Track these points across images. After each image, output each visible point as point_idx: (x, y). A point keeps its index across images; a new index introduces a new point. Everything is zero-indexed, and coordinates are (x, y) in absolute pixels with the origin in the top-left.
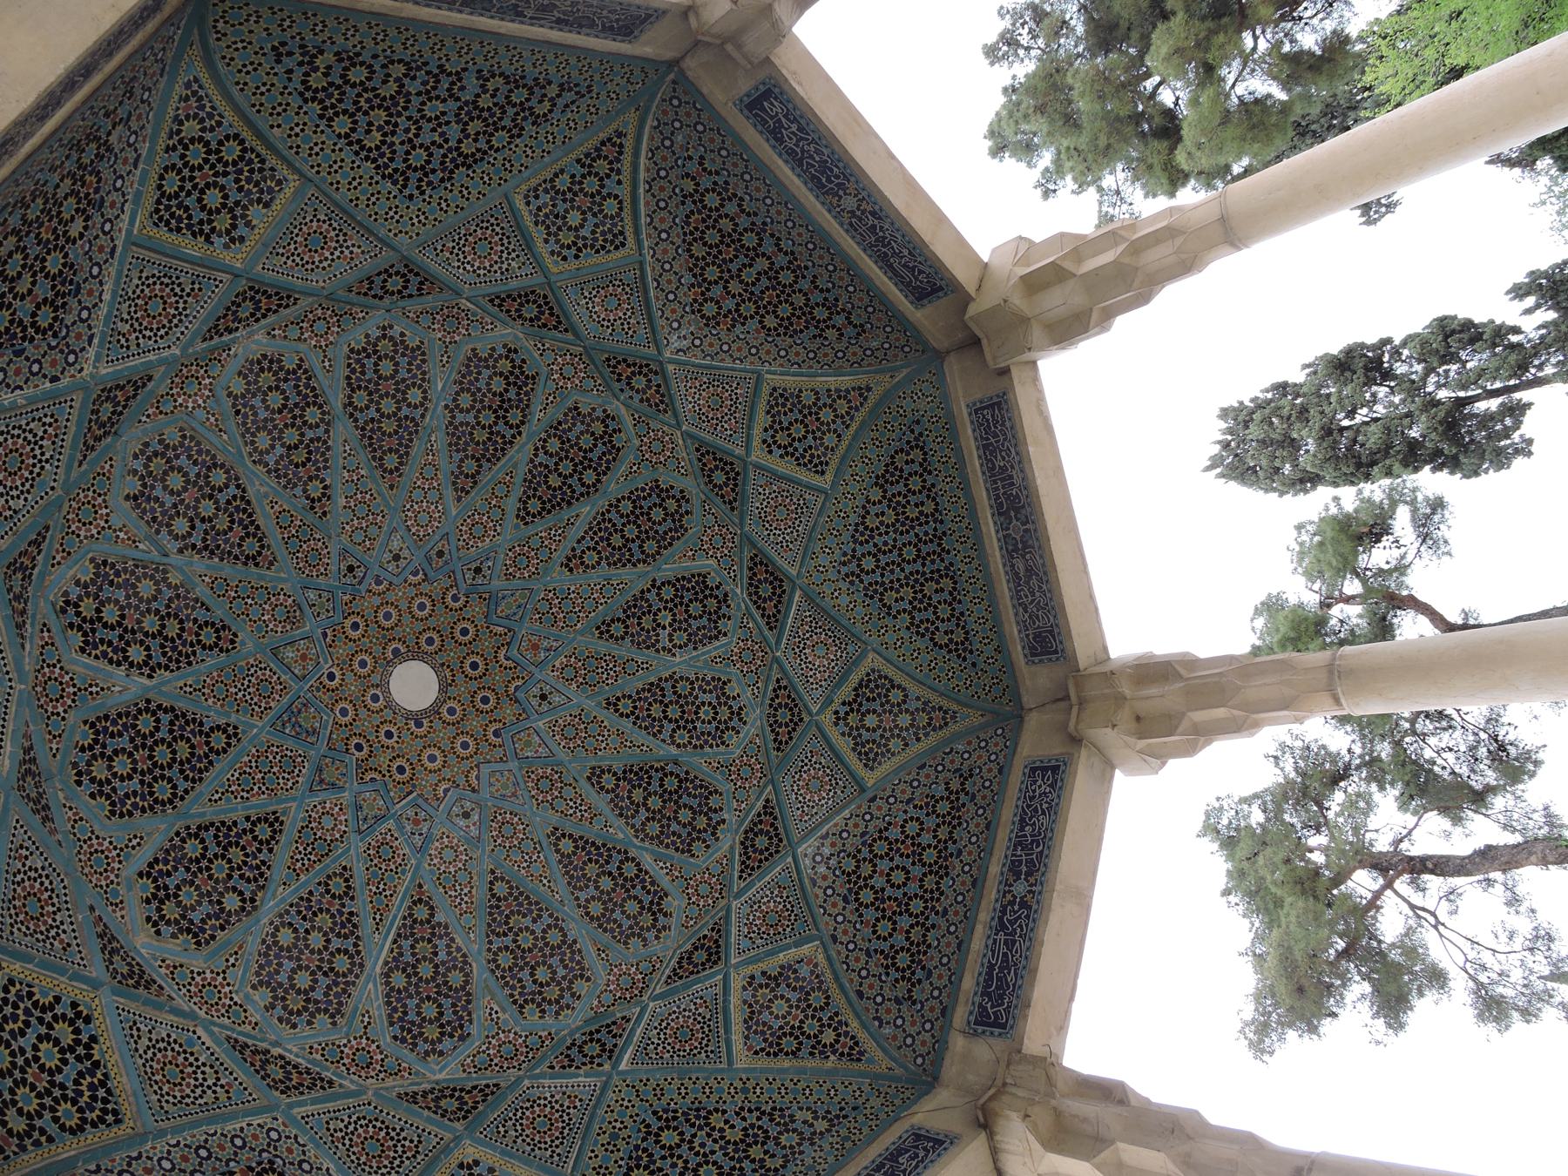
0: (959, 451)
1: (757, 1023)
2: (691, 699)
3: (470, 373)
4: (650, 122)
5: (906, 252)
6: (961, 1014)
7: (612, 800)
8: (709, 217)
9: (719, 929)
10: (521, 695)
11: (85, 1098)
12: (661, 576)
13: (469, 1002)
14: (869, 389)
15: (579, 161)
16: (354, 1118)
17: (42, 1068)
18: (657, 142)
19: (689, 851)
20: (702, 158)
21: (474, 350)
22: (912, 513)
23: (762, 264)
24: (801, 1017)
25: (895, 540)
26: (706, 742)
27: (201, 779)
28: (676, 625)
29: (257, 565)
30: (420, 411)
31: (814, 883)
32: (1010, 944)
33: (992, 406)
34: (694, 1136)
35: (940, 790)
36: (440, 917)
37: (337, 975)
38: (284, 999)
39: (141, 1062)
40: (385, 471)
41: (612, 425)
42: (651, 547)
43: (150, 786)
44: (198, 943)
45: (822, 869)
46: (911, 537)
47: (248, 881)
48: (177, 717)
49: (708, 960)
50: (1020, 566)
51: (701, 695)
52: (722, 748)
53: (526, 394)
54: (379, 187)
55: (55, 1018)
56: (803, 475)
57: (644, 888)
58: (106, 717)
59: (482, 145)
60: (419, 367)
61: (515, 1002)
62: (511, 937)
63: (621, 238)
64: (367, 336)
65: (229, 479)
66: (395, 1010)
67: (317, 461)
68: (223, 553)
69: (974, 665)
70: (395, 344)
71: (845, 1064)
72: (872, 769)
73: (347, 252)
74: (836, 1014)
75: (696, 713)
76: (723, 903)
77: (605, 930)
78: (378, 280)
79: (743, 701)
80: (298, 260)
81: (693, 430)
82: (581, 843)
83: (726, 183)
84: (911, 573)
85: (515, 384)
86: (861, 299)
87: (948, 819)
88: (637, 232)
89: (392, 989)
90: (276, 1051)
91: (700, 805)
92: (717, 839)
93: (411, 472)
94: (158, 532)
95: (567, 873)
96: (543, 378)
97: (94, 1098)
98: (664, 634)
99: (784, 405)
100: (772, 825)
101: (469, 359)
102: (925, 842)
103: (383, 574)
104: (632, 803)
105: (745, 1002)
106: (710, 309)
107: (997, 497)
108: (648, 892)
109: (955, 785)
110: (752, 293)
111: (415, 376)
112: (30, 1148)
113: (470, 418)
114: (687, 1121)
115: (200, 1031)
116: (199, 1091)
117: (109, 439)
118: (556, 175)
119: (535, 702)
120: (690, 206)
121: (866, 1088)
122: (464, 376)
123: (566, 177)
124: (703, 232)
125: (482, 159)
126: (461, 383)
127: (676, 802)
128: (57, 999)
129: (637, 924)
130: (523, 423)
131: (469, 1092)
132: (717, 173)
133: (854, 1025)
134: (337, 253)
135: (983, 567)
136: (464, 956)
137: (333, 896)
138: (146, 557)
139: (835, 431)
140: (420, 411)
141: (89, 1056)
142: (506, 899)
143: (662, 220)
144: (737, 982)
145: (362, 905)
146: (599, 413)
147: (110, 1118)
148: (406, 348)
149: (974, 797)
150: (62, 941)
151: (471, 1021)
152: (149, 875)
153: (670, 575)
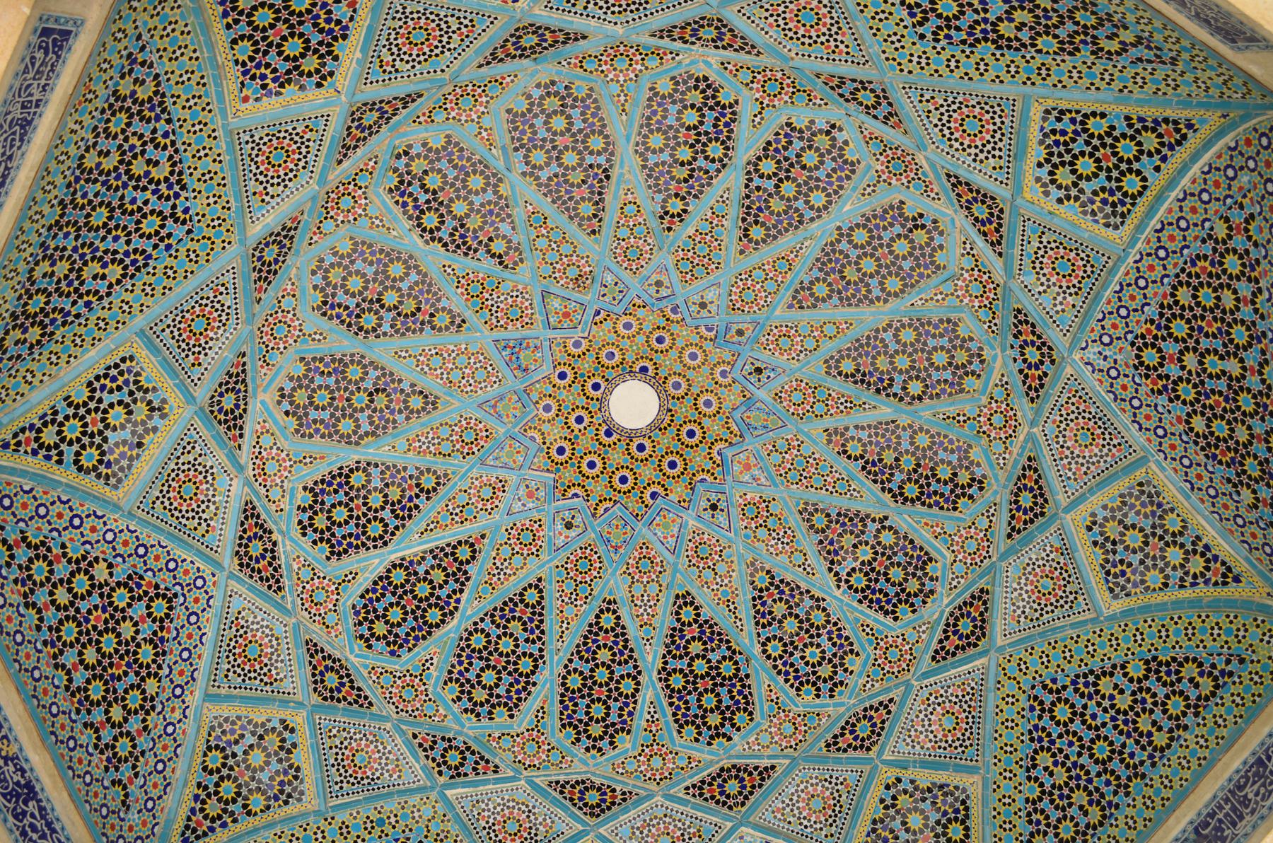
4: (1228, 140)
7: (674, 629)
8: (1219, 277)
14: (1237, 579)
15: (1128, 118)
17: (103, 420)
18: (1222, 163)
19: (681, 726)
20: (1252, 216)
21: (902, 202)
22: (1144, 724)
23: (1233, 367)
25: (1104, 725)
26: (787, 673)
29: (580, 225)
30: (813, 214)
36: (472, 569)
37: (364, 533)
38: (316, 513)
39: (173, 466)
40: (746, 236)
44: (297, 431)
46: (1118, 740)
47: (371, 423)
48: (423, 282)
49: (592, 807)
51: (825, 637)
52: (793, 691)
53: (921, 275)
54: (893, 9)
57: (621, 709)
58: (370, 246)
59: (1025, 36)
61: (450, 672)
63: (1119, 220)
64: (812, 122)
65: (605, 150)
70: (833, 146)
75: (805, 645)
76: (652, 786)
77: (562, 702)
79: (850, 680)
82: (619, 630)
83: (1258, 262)
84: (1082, 767)
85: (917, 259)
89: (388, 578)
90: (274, 537)
91: (728, 708)
92: (709, 744)
93: (768, 253)
94: (516, 149)
96: (946, 274)
99: (1143, 505)
100: (753, 787)
101: (892, 207)
103: (683, 308)
104: (686, 648)
106: (1150, 356)
107: (1212, 815)
110: (1202, 382)
111: (831, 184)
113: (853, 254)
118: (1094, 114)
119: (705, 504)
120: (1207, 249)
122: (875, 217)
123: (1105, 124)
124: (1201, 284)
125: (1017, 49)
126: (868, 220)
127: (715, 685)
130: (896, 295)
132: (1256, 244)
134: (823, 39)
136: (456, 608)
138: (492, 162)
139: (1167, 577)
142: (527, 606)
143: (1172, 238)
145: (430, 509)
146: (973, 346)
148: (841, 156)
152: (307, 364)
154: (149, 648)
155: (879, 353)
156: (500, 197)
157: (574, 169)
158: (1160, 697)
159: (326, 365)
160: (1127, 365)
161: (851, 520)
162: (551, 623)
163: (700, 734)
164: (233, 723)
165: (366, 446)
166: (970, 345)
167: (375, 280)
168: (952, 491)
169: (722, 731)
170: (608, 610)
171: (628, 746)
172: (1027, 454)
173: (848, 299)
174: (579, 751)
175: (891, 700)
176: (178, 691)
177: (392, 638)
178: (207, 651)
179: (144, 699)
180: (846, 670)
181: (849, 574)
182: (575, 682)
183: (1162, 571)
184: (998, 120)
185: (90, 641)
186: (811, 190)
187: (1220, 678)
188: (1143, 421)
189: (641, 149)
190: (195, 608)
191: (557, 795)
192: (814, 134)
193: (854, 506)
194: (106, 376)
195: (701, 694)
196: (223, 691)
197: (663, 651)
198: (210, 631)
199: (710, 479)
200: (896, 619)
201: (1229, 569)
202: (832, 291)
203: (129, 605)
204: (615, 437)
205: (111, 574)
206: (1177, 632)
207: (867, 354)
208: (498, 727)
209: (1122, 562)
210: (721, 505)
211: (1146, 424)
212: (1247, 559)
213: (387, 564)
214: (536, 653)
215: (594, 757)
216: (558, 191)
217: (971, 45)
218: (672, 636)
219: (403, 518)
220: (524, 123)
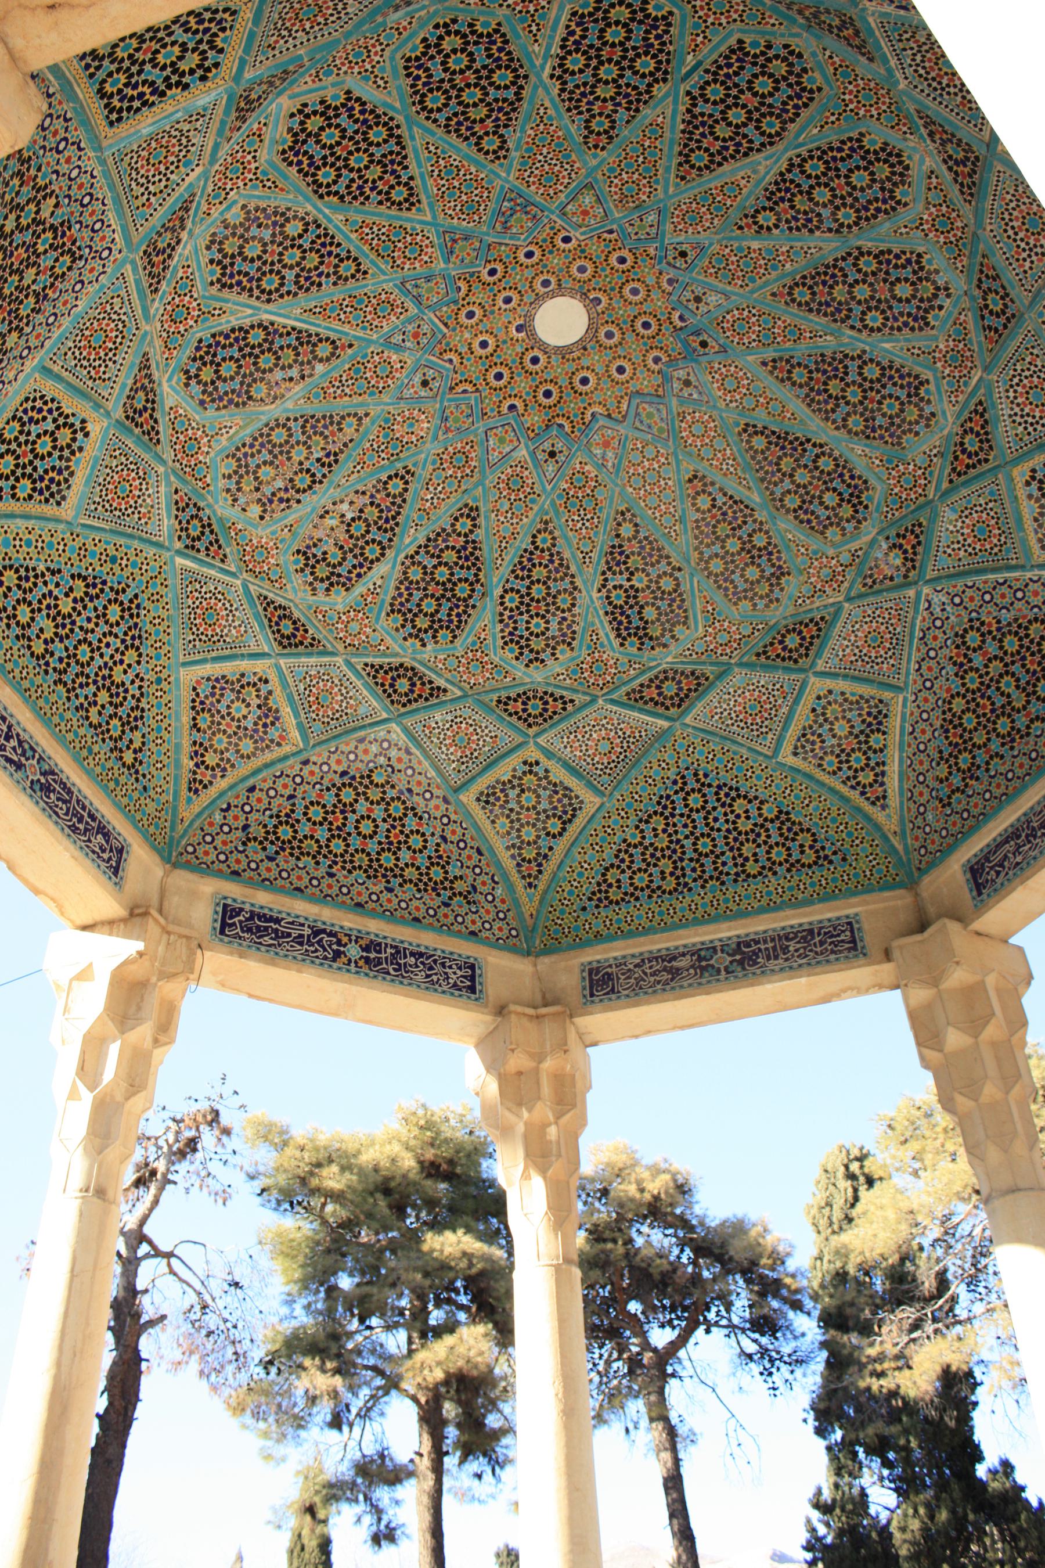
0: (808, 902)
2: (552, 608)
3: (902, 377)
5: (1019, 859)
6: (234, 891)
10: (554, 431)
22: (747, 850)
24: (230, 731)
25: (719, 830)
28: (632, 593)
29: (680, 164)
30: (858, 325)
31: (362, 740)
32: (299, 940)
33: (853, 941)
35: (454, 870)
37: (259, 280)
42: (716, 566)
43: (439, 89)
44: (284, 152)
45: (374, 748)
46: (721, 846)
47: (348, 187)
48: (512, 103)
50: (683, 963)
52: (501, 642)
53: (882, 437)
56: (793, 732)
57: (354, 567)
58: (506, 42)
60: (906, 324)
61: (238, 449)
64: (937, 272)
65: (770, 136)
66: (227, 337)
68: (691, 133)
69: (584, 909)
70: (929, 300)
71: (186, 776)
72: (478, 800)
73: (1024, 255)
74: (233, 766)
76: (340, 647)
78: (995, 285)
80: (1013, 205)
81: (844, 615)
86: (976, 806)
87: (425, 879)
89: (247, 332)
90: (184, 235)
93: (792, 315)
94: (707, 71)
97: (132, 99)
98: (621, 580)
99: (869, 714)
101: (917, 377)
102: (400, 854)
105: (243, 675)
107: (757, 942)
109: (460, 886)
110: (988, 687)
111: (896, 319)
117: (802, 21)
119: (547, 446)
121: (164, 798)
122: (898, 371)
128: (221, 51)
130: (849, 432)
133: (221, 784)
134: (1023, 245)
135: (683, 923)
137: (336, 266)
140: (858, 325)
141: (169, 87)
144: (260, 666)
145: (330, 293)
147: (114, 116)
148: (926, 311)
149: (447, 905)
151: (218, 409)
152: (349, 99)
154: (32, 300)
156: (648, 92)
157: (729, 124)
158: (772, 841)
159: (362, 112)
164: (46, 403)
165: (329, 206)
167: (477, 71)
169: (422, 635)
172: (824, 613)
174: (298, 580)
178: (66, 322)
186: (877, 308)
187: (822, 859)
188: (924, 668)
191: (260, 609)
193: (662, 542)
196: (56, 369)
197: (422, 541)
199: (568, 428)
202: (807, 384)
206: (817, 808)
210: (561, 458)
211: (923, 671)
212: (901, 803)
213: (255, 320)
214: (319, 476)
216: (696, 128)
219: (300, 288)
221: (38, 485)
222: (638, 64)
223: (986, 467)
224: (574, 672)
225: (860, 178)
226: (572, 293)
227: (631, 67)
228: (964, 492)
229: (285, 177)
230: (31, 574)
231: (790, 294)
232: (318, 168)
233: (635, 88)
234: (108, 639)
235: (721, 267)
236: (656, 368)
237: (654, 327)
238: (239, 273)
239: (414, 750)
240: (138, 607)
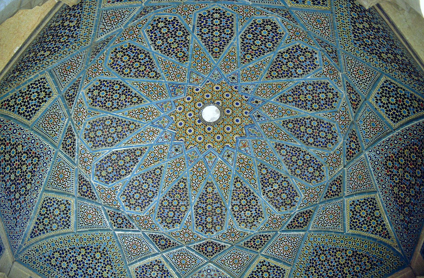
1: (146, 269)
3: (320, 85)
7: (204, 193)
9: (175, 246)
10: (226, 148)
11: (30, 110)
12: (289, 179)
13: (118, 179)
16: (67, 167)
17: (30, 97)
21: (328, 83)
27: (137, 77)
28: (275, 191)
29: (212, 54)
30: (296, 75)
31: (200, 272)
34: (101, 263)
36: (140, 159)
37: (106, 141)
38: (91, 132)
41: (333, 141)
42: (298, 172)
44: (92, 104)
45: (205, 273)
48: (150, 61)
49: (162, 246)
55: (44, 91)
61: (124, 192)
62: (144, 181)
63: (396, 120)
64: (307, 48)
65: (230, 34)
67: (257, 53)
68: (208, 44)
70: (311, 58)
75: (247, 210)
77: (159, 209)
80: (309, 19)
81: (346, 173)
85: (326, 102)
88: (402, 126)
90: (75, 137)
91: (215, 223)
92: (206, 233)
94: (198, 26)
95: (173, 189)
96: (335, 110)
97: (31, 111)
98: (269, 188)
100: (217, 251)
101: (324, 83)
104: (206, 200)
105: (151, 262)
108: (178, 217)
110: (402, 179)
111: (306, 68)
112: (8, 109)
114: (105, 259)
115: (67, 119)
116: (51, 129)
119: (226, 154)
126: (315, 84)
127: (213, 215)
129: (166, 218)
130: (315, 110)
131: (91, 192)
136: (131, 171)
137: (128, 127)
142: (155, 175)
144: (157, 257)
145: (130, 136)
148: (313, 61)
150: (65, 79)
151: (112, 182)
153: (291, 183)
155: (302, 125)
156: (187, 40)
160: (381, 163)
161: (275, 174)
162: (162, 183)
163: (203, 229)
164: (51, 200)
165: (114, 112)
166: (334, 134)
167: (133, 58)
168: (311, 176)
170: (183, 182)
171: (178, 228)
172: (340, 174)
173: (298, 105)
174: (161, 226)
175: (269, 236)
176: (36, 188)
177: (107, 177)
179: (26, 191)
180: (258, 222)
181: (268, 192)
182: (165, 203)
183: (368, 226)
184: (370, 75)
185: (13, 171)
186: (298, 68)
189: (243, 37)
190: (46, 161)
192: (306, 52)
194: (34, 84)
195: (207, 217)
196: (50, 189)
198: (49, 169)
200: (279, 210)
201: (388, 234)
202: (294, 100)
203: (26, 160)
204: (201, 123)
205: (22, 149)
207: (298, 124)
208: (137, 213)
209: (357, 219)
215: (166, 229)
216: (208, 42)
217: (370, 53)
218: (203, 195)
220: (204, 19)
221: (59, 224)
222: (177, 34)
223: (361, 102)
224: (267, 225)
225: (265, 33)
226: (209, 104)
227: (176, 36)
228: (360, 114)
229: (97, 110)
230: (64, 251)
231: (271, 75)
232: (105, 103)
233: (182, 41)
234: (98, 264)
235: (246, 77)
236: (247, 115)
237: (235, 104)
238: (99, 141)
239: (220, 270)
240: (106, 251)
